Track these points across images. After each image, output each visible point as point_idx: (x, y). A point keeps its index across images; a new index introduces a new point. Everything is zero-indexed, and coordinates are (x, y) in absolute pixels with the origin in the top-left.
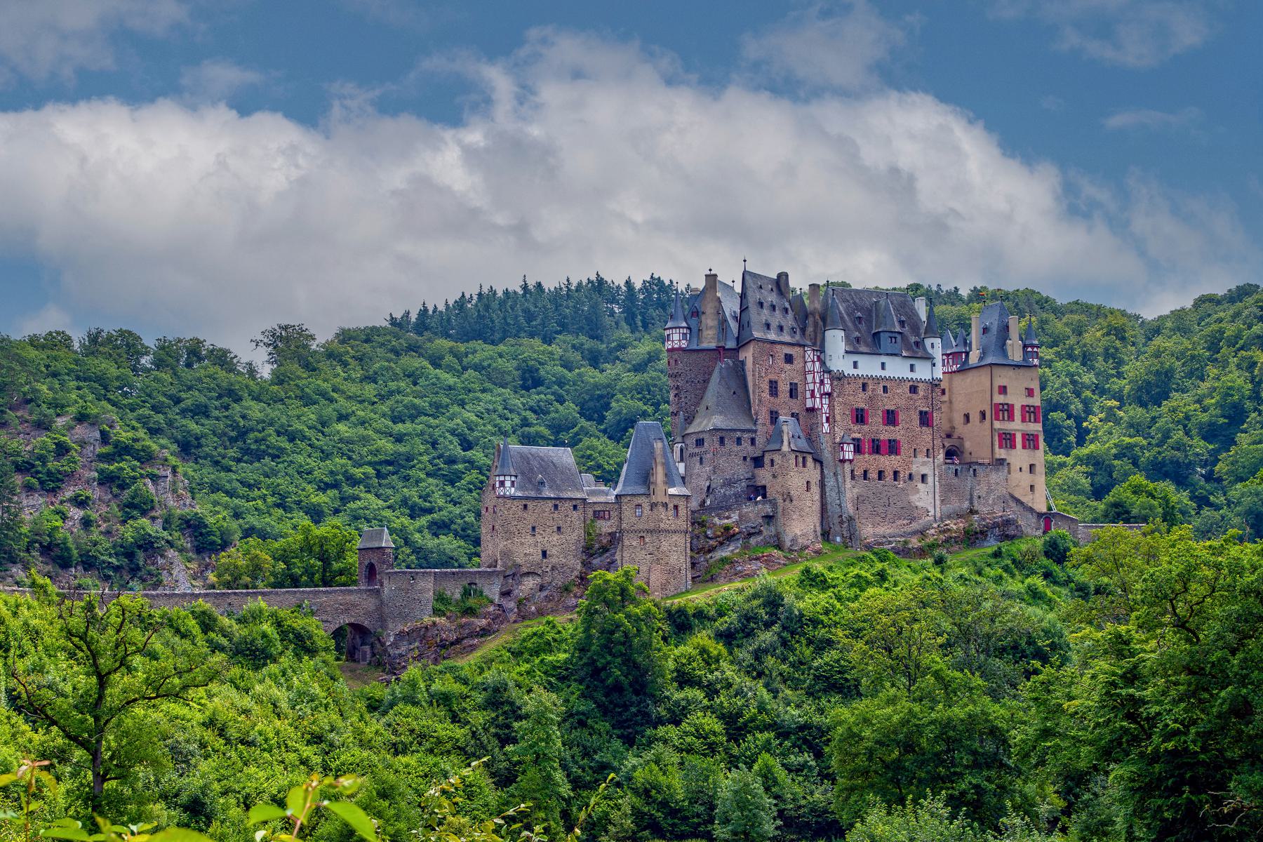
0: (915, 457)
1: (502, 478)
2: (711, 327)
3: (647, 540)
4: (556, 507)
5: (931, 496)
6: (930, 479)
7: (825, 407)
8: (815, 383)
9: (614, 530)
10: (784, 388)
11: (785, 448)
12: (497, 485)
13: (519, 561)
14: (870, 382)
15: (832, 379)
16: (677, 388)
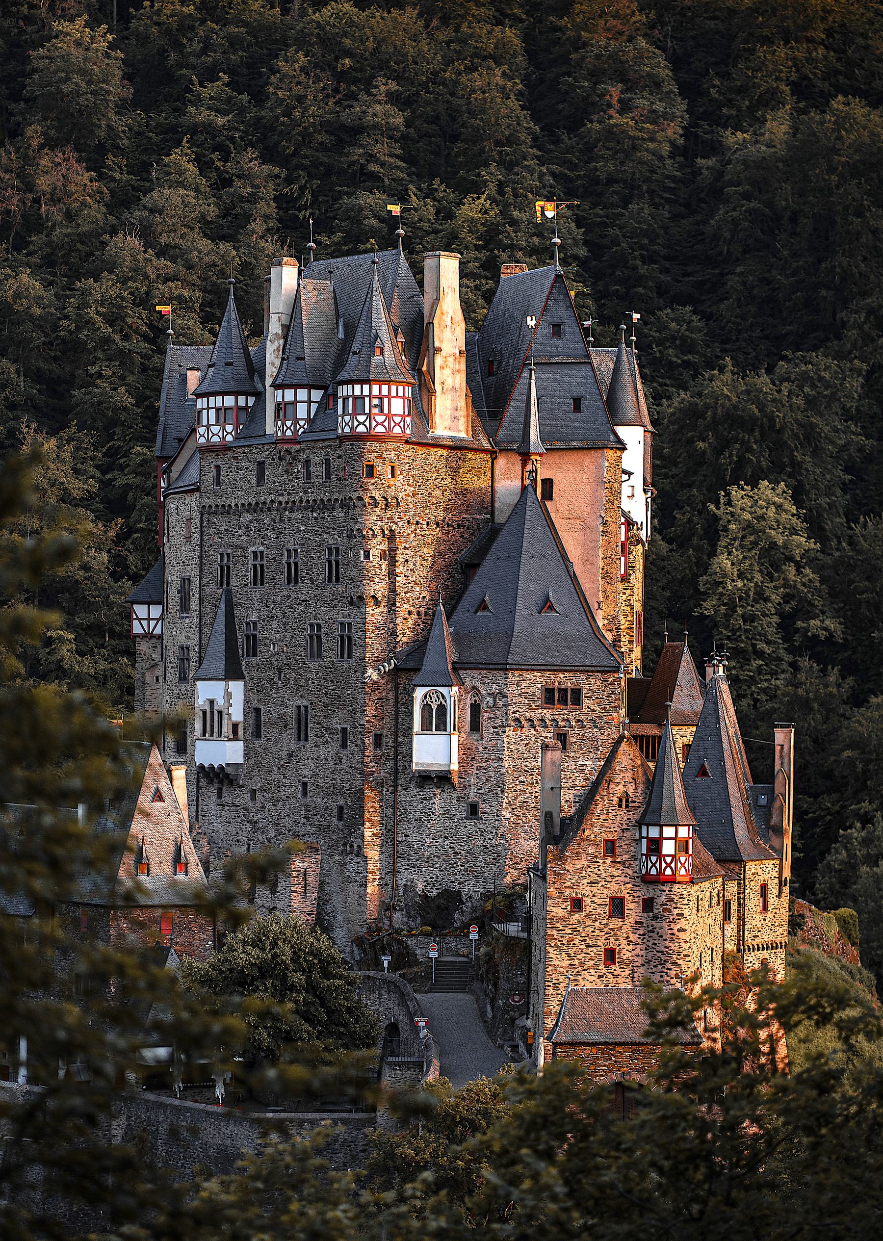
12: (668, 848)
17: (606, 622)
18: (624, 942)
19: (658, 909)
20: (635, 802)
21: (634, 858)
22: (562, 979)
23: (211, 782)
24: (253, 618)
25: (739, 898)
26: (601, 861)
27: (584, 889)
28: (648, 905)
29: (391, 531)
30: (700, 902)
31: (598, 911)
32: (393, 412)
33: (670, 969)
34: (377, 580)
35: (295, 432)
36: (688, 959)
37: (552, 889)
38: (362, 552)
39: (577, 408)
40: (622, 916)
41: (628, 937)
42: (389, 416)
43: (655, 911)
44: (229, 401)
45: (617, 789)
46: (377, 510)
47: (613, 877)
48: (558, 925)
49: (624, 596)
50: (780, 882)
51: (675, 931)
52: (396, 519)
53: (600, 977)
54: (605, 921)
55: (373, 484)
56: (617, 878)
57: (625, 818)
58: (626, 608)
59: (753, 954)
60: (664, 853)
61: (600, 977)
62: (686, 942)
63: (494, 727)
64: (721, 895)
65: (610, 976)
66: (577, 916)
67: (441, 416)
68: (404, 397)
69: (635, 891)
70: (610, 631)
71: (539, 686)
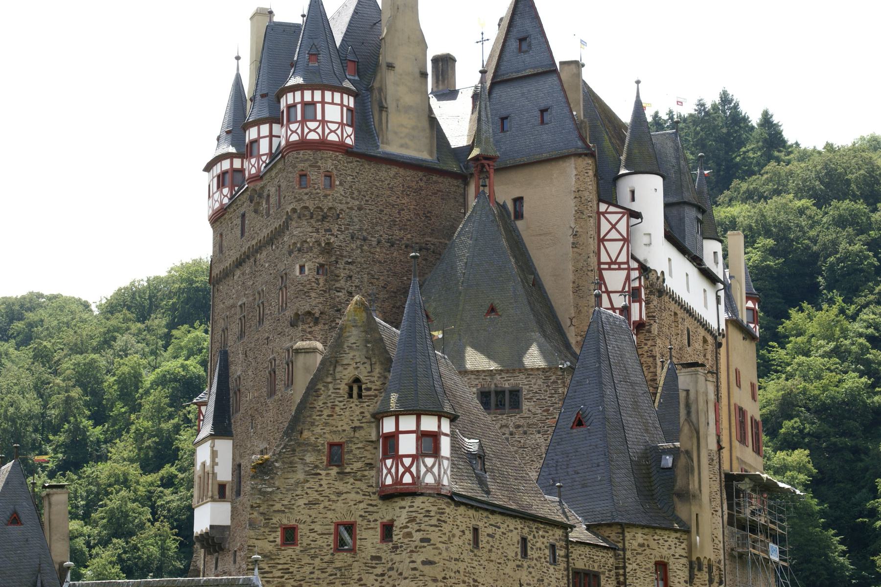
1: (429, 424)
2: (408, 109)
12: (407, 445)
16: (328, 249)
17: (579, 338)
19: (397, 536)
20: (369, 389)
21: (370, 466)
23: (210, 553)
24: (239, 373)
25: (617, 575)
26: (323, 473)
27: (299, 515)
28: (387, 530)
29: (328, 244)
30: (483, 538)
31: (319, 543)
32: (327, 119)
34: (313, 295)
35: (259, 168)
37: (256, 514)
38: (298, 267)
39: (542, 122)
40: (352, 550)
41: (360, 580)
42: (323, 122)
43: (395, 538)
44: (226, 165)
45: (346, 372)
46: (312, 221)
47: (339, 494)
49: (646, 348)
50: (691, 563)
51: (418, 565)
54: (327, 558)
55: (306, 194)
56: (344, 496)
57: (358, 413)
58: (648, 359)
60: (400, 453)
64: (561, 552)
66: (289, 551)
67: (396, 133)
68: (342, 105)
71: (475, 390)
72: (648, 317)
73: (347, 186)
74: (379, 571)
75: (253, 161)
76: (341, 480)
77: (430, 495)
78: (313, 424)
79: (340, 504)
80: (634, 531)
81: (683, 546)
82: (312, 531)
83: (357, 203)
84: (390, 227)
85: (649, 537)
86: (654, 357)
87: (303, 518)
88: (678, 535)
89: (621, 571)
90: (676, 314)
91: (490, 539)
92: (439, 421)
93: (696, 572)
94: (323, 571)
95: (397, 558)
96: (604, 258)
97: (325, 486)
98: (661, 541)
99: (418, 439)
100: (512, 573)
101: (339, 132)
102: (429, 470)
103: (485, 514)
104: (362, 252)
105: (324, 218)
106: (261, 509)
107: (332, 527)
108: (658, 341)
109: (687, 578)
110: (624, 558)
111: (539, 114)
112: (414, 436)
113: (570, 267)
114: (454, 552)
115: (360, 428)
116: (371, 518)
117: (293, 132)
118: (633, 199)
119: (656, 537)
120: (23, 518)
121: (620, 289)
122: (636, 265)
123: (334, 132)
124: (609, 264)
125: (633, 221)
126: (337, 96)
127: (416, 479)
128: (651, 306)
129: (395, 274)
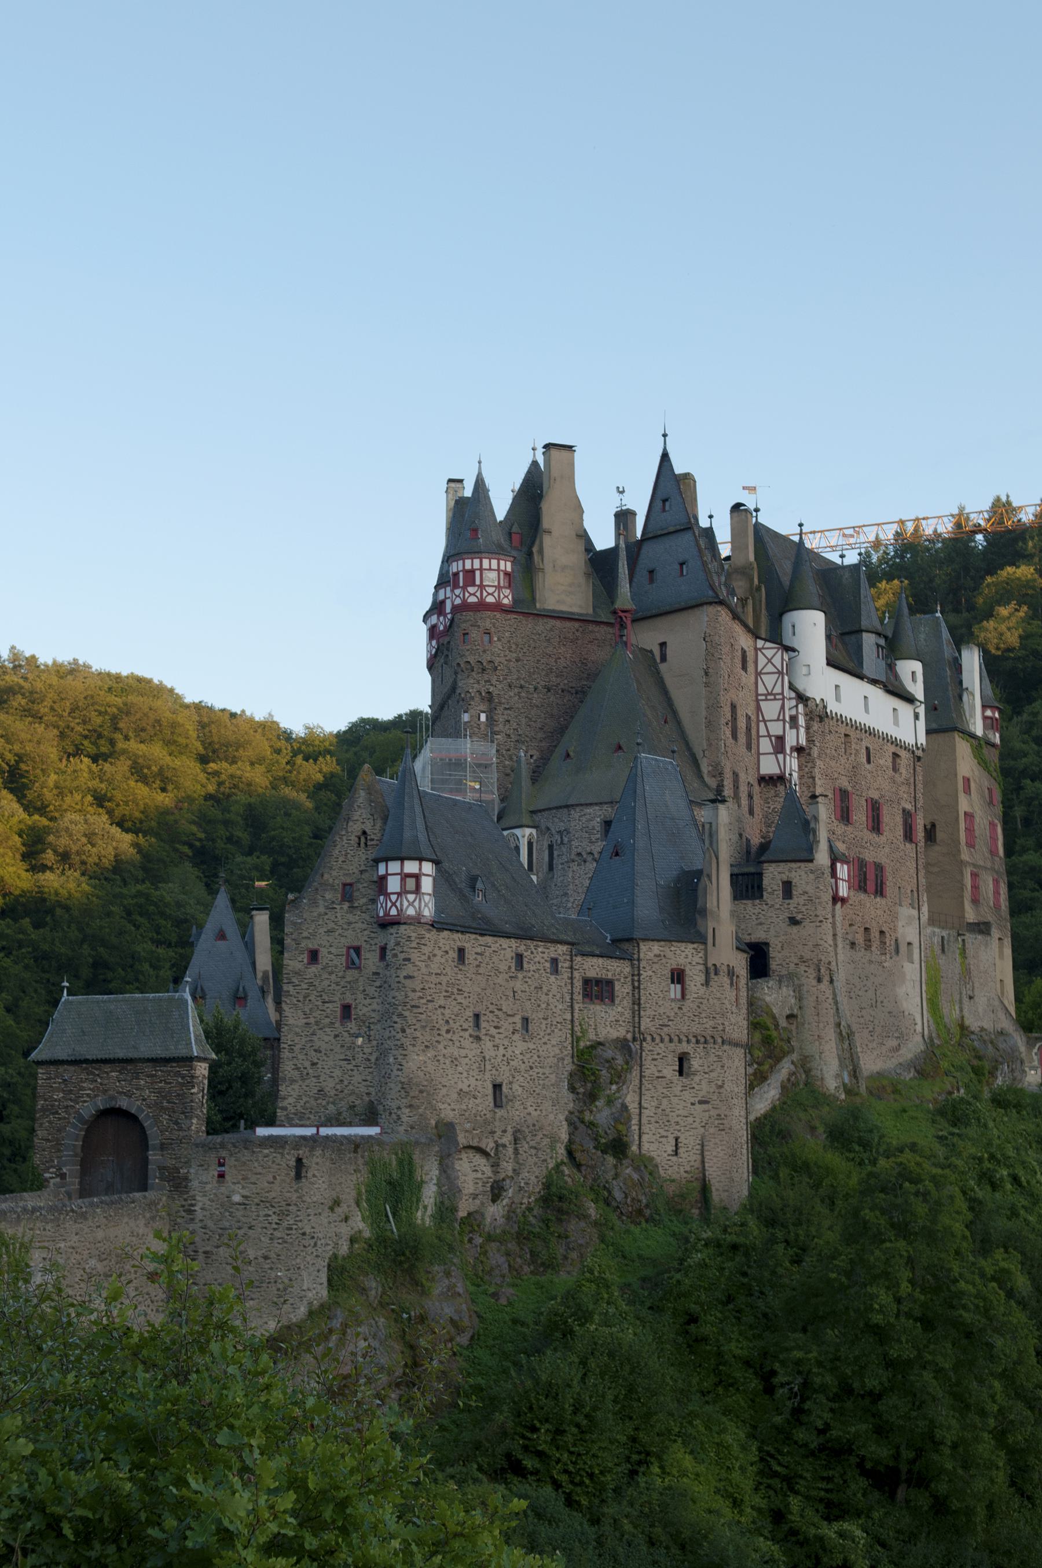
0: (901, 905)
2: (564, 568)
3: (695, 1063)
4: (519, 958)
5: (918, 984)
6: (916, 952)
7: (795, 775)
8: (784, 720)
9: (620, 1032)
10: (742, 724)
11: (822, 857)
12: (393, 884)
13: (448, 1113)
14: (852, 733)
15: (810, 716)
16: (489, 698)
17: (710, 768)
18: (360, 996)
20: (372, 840)
22: (297, 1039)
25: (633, 980)
30: (470, 956)
31: (335, 962)
33: (396, 1023)
36: (415, 1010)
37: (289, 940)
40: (359, 968)
41: (364, 991)
42: (482, 587)
45: (355, 826)
46: (474, 674)
47: (350, 923)
48: (294, 980)
50: (707, 969)
52: (494, 682)
53: (336, 1036)
54: (340, 974)
56: (353, 926)
59: (661, 1045)
60: (389, 891)
61: (336, 1036)
62: (414, 991)
63: (562, 864)
65: (346, 1034)
66: (313, 969)
68: (498, 570)
69: (372, 938)
70: (714, 776)
72: (810, 740)
73: (504, 641)
74: (378, 984)
75: (441, 618)
76: (351, 912)
77: (410, 924)
78: (331, 868)
79: (350, 931)
80: (651, 943)
81: (701, 955)
82: (330, 953)
83: (515, 655)
84: (547, 675)
85: (667, 949)
86: (813, 778)
87: (325, 943)
88: (695, 946)
89: (636, 978)
90: (846, 735)
91: (479, 957)
92: (420, 865)
93: (712, 975)
94: (337, 984)
95: (388, 973)
96: (761, 690)
97: (339, 918)
98: (678, 952)
99: (402, 879)
100: (503, 983)
101: (496, 594)
102: (411, 904)
103: (473, 936)
104: (520, 698)
105: (484, 670)
106: (293, 936)
107: (345, 950)
108: (818, 763)
109: (703, 982)
110: (639, 967)
111: (678, 567)
112: (399, 877)
113: (704, 705)
114: (435, 968)
115: (366, 871)
116: (372, 942)
117: (457, 596)
118: (794, 634)
119: (673, 949)
120: (228, 936)
121: (776, 718)
122: (793, 695)
123: (492, 594)
124: (766, 695)
125: (792, 654)
126: (494, 562)
127: (400, 911)
128: (811, 731)
129: (552, 716)
